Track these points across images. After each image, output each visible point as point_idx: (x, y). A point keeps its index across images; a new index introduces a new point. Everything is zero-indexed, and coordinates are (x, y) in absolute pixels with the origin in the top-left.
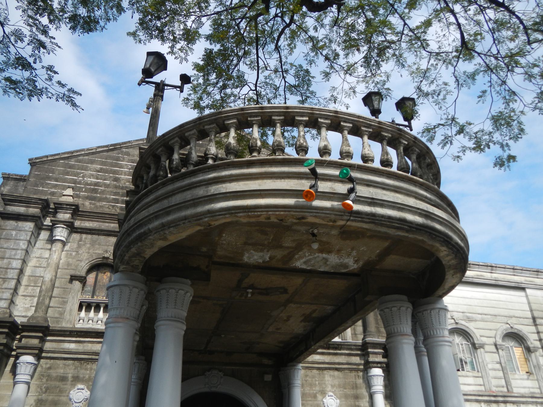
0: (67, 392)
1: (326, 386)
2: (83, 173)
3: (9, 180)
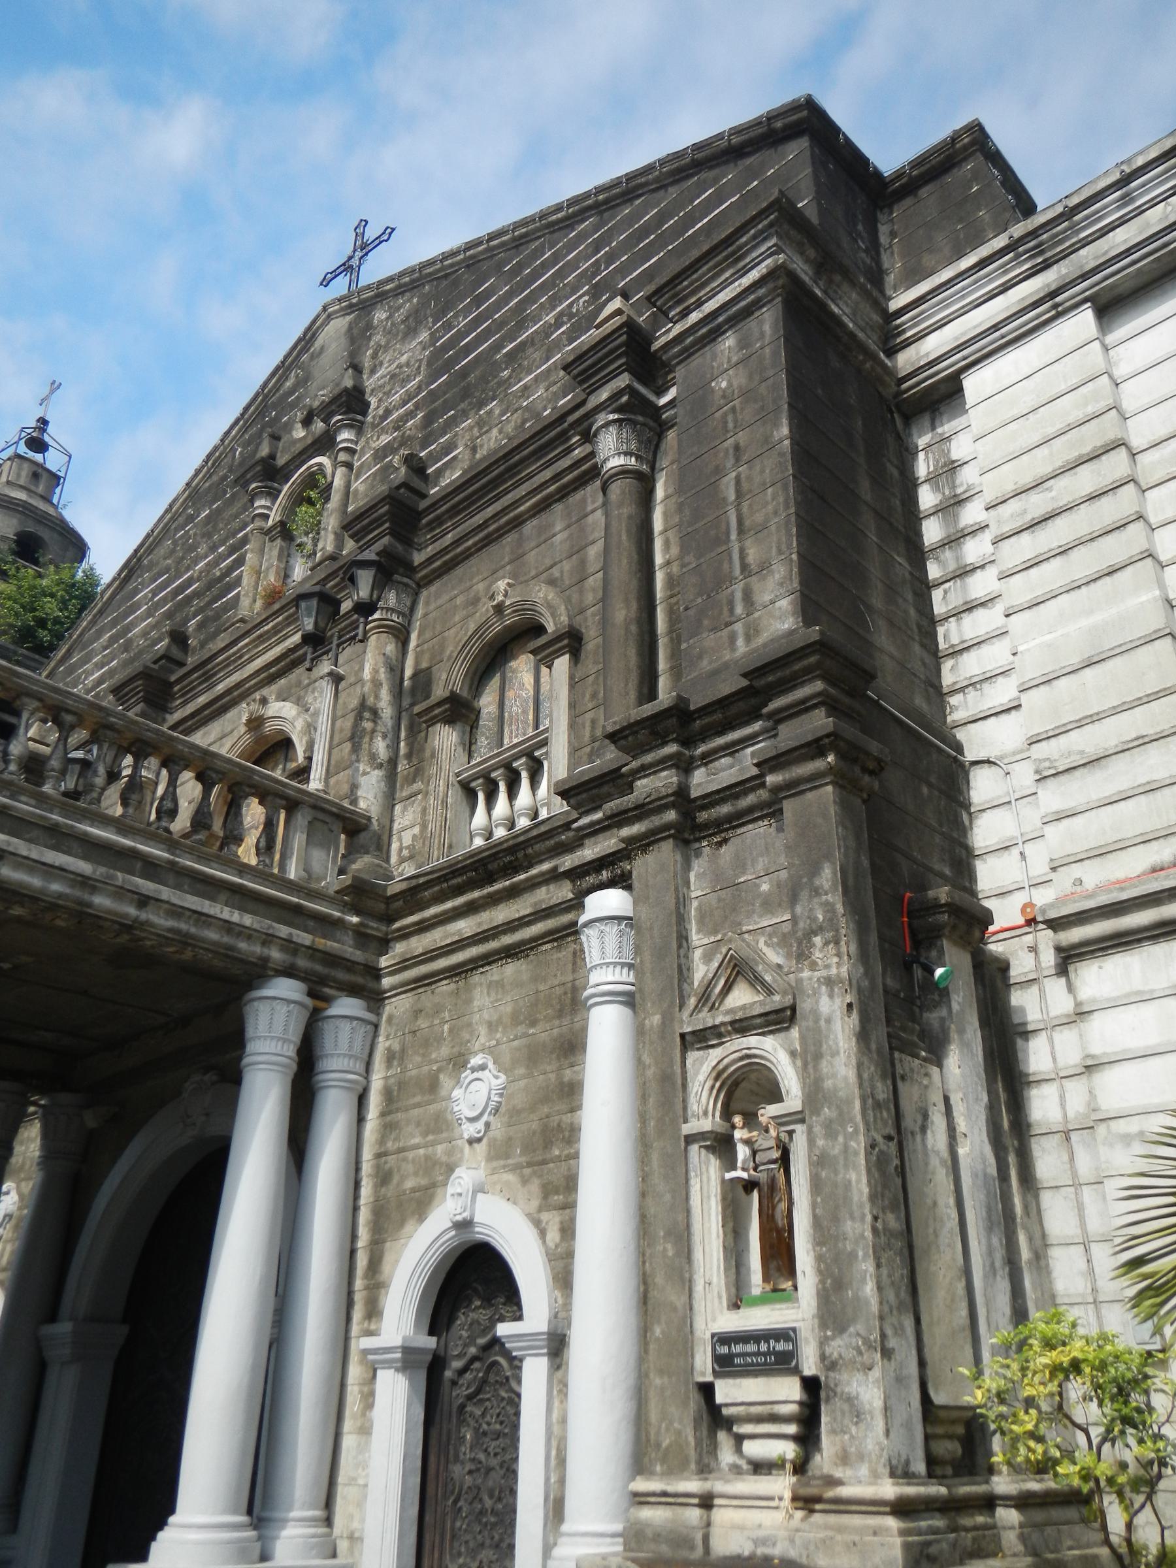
1: (472, 1033)
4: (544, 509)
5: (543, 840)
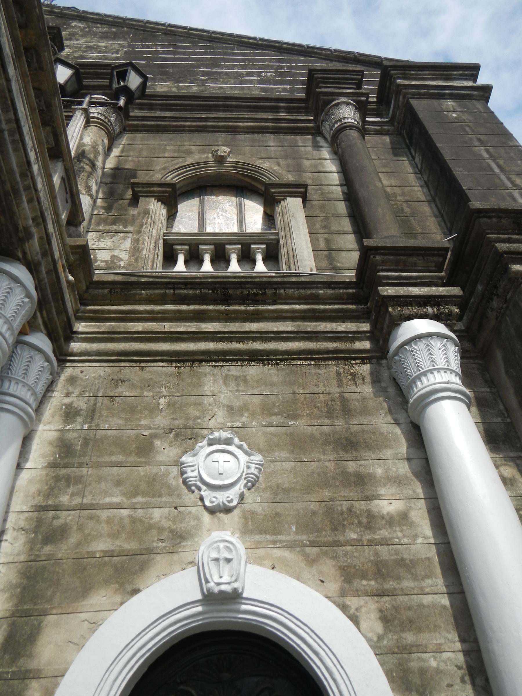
4: (258, 133)
5: (298, 288)
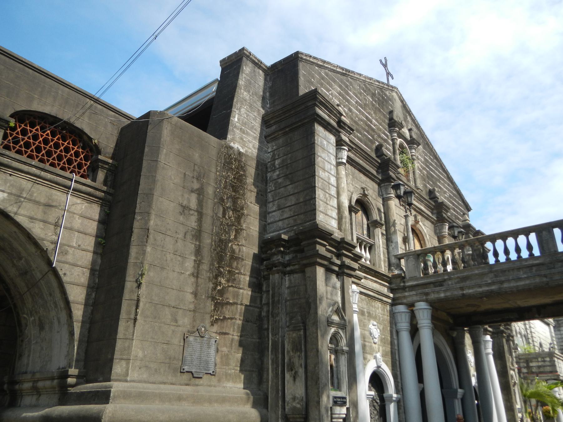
0: (367, 326)
2: (331, 91)
3: (248, 60)
